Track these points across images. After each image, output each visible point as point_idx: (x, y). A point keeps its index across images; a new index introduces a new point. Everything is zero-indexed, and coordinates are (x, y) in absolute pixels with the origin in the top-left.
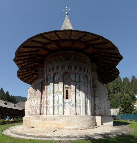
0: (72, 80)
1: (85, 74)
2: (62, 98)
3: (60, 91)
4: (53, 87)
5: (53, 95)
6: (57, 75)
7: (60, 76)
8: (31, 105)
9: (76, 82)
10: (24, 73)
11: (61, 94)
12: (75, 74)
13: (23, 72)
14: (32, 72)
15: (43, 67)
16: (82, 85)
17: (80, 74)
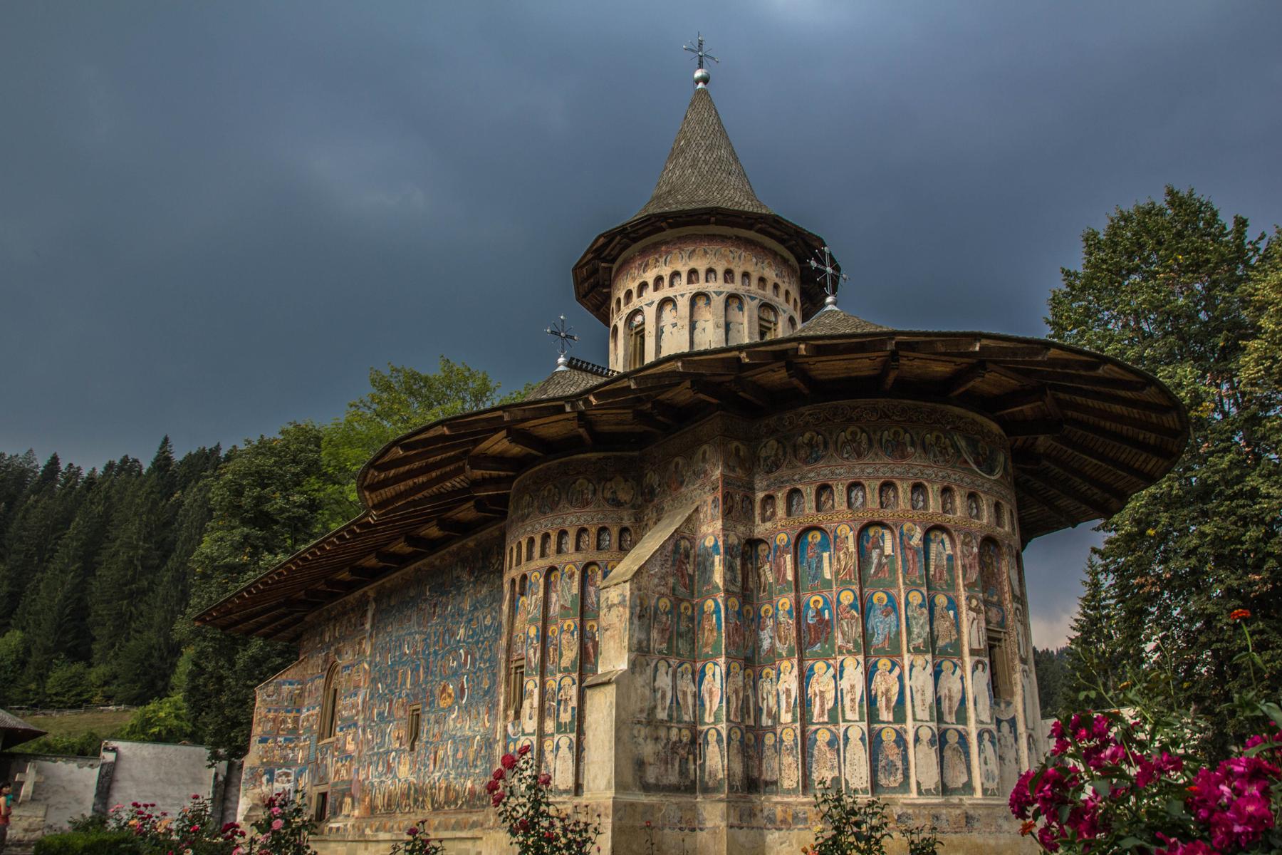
3: (976, 646)
5: (929, 669)
8: (655, 707)
11: (980, 666)
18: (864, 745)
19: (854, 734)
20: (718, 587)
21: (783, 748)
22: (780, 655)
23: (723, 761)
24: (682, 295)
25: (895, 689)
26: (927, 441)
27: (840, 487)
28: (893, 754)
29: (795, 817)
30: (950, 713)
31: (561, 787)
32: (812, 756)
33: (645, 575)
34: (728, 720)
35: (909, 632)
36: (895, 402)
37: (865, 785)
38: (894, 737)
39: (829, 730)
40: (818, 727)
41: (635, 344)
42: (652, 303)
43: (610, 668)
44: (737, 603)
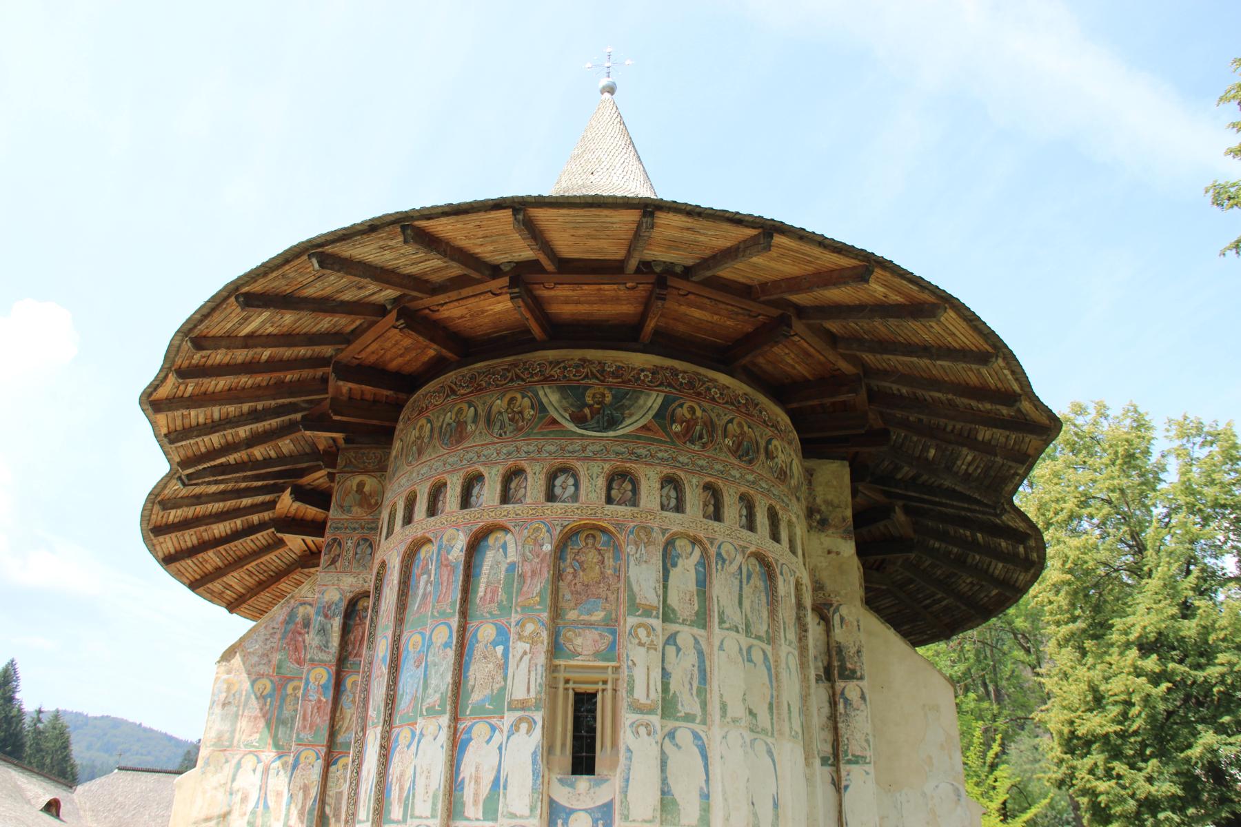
0: (632, 598)
1: (753, 549)
2: (534, 762)
3: (519, 693)
4: (451, 654)
5: (443, 736)
6: (504, 547)
7: (525, 559)
9: (668, 615)
10: (200, 510)
11: (524, 726)
12: (670, 543)
13: (198, 499)
14: (271, 505)
15: (381, 469)
16: (721, 648)
17: (713, 551)
26: (494, 409)
30: (475, 802)
36: (464, 370)
44: (326, 676)
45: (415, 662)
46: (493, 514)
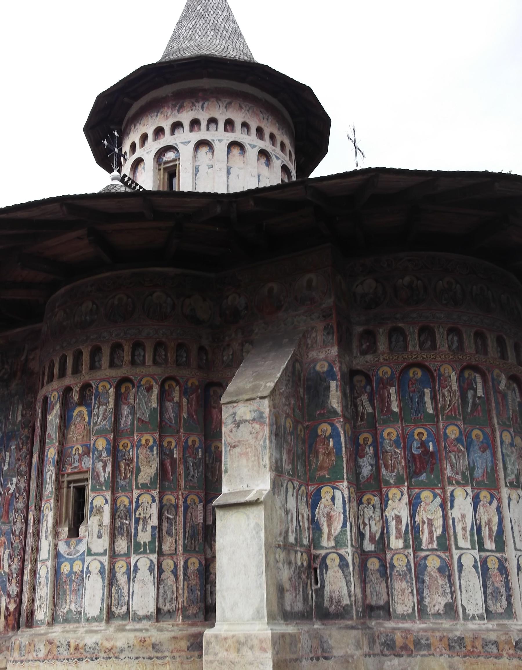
6: (514, 390)
18: (477, 572)
19: (468, 561)
20: (335, 412)
21: (395, 573)
22: (387, 483)
23: (348, 587)
24: (220, 141)
25: (495, 520)
27: (441, 330)
28: (497, 581)
29: (417, 643)
31: (141, 613)
32: (423, 582)
33: (277, 392)
34: (352, 545)
35: (505, 468)
37: (480, 611)
38: (497, 566)
39: (439, 556)
40: (427, 553)
41: (163, 178)
42: (189, 142)
43: (242, 487)
45: (480, 448)
46: (516, 369)
